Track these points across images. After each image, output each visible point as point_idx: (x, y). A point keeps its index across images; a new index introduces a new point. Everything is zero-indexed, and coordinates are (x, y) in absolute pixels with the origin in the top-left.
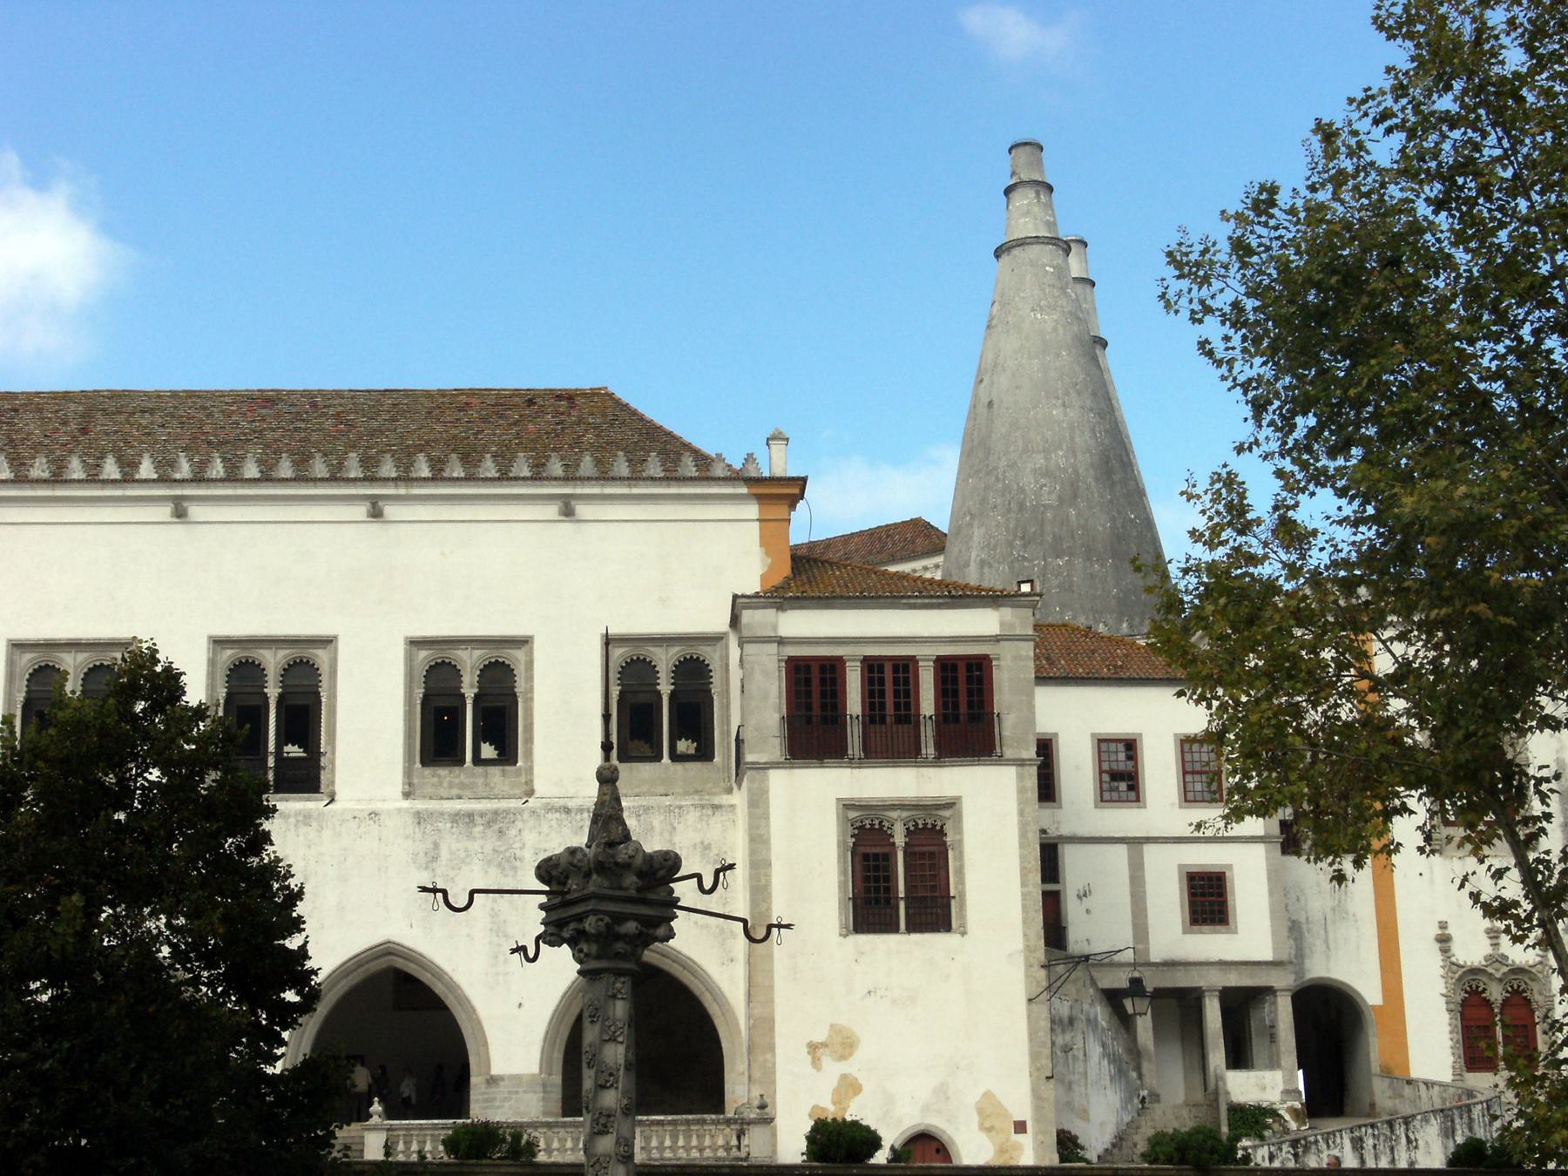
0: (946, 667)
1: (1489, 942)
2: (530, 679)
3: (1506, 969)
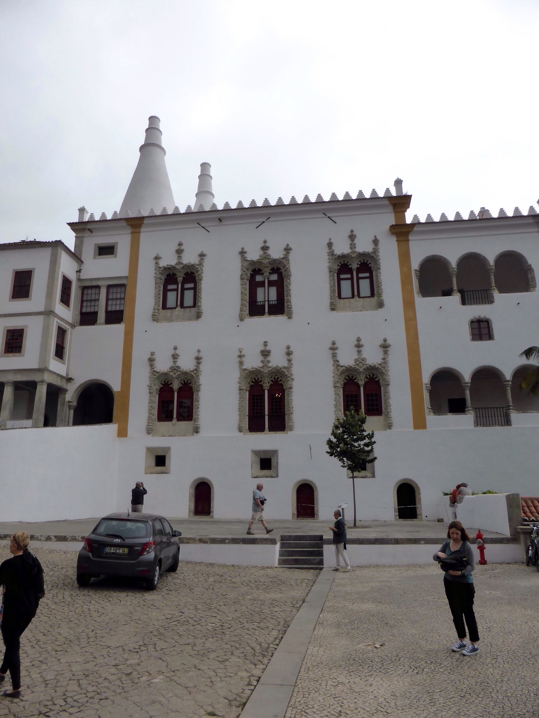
1: (172, 360)
3: (179, 373)
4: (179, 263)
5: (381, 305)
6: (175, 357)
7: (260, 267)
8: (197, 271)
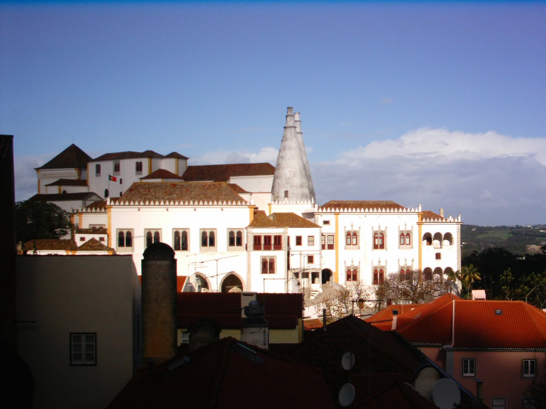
0: (275, 237)
5: (412, 248)
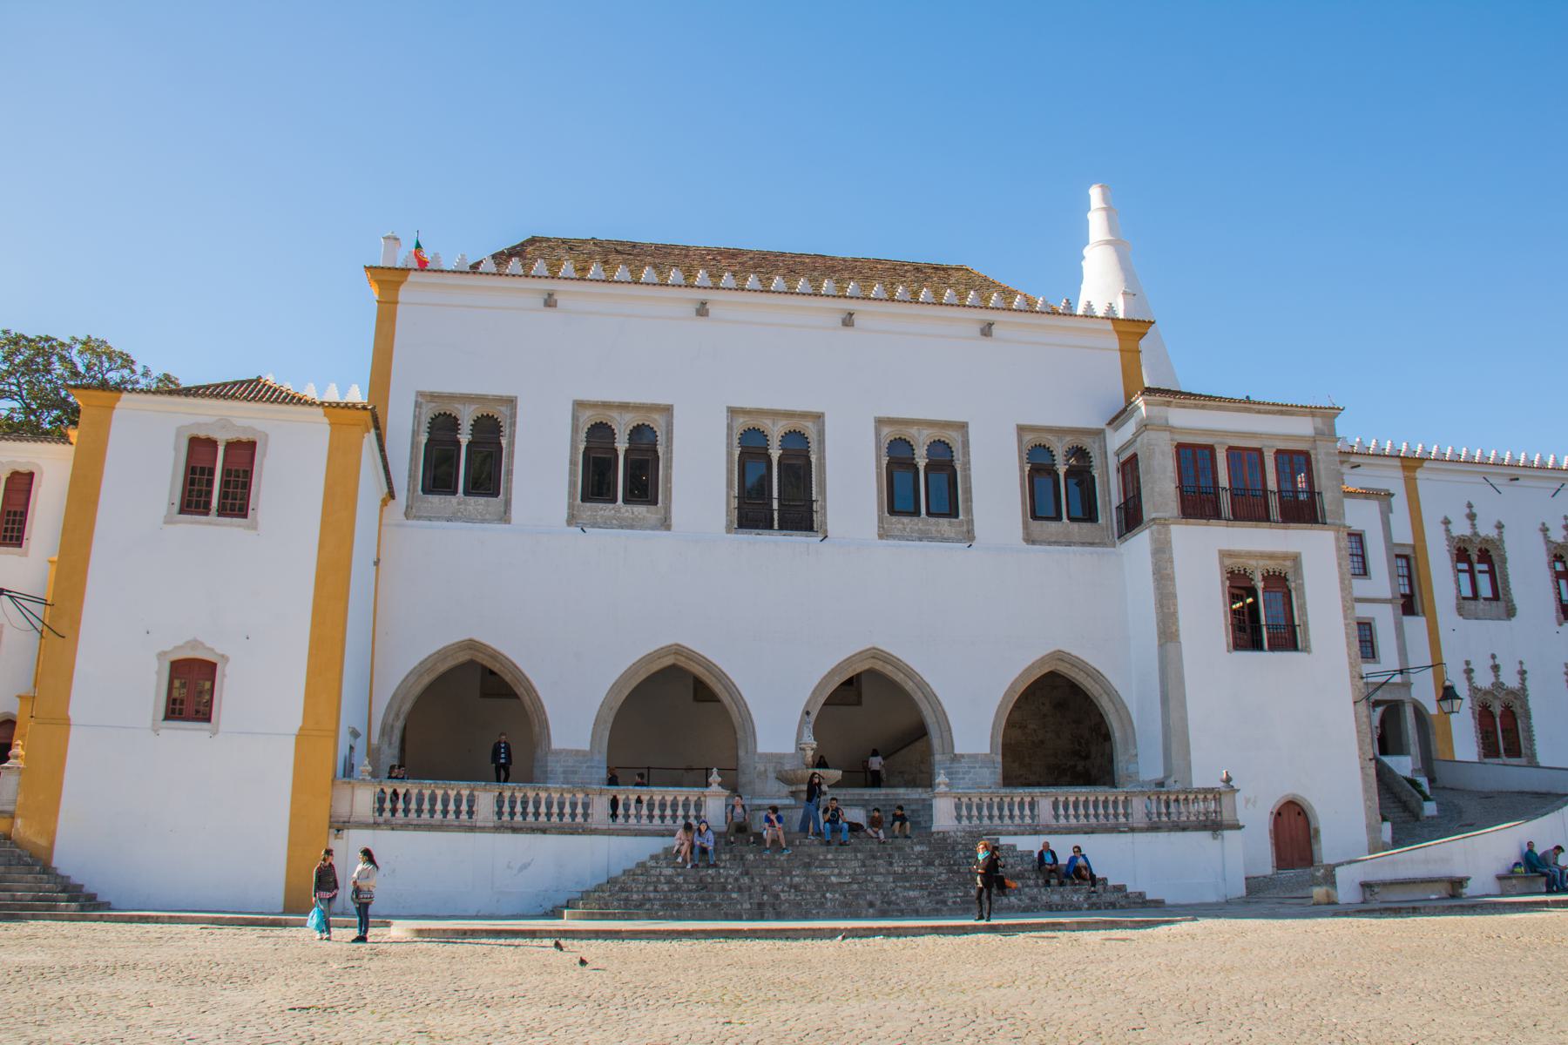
2: (966, 453)
4: (1476, 534)
6: (1496, 668)
7: (1563, 553)
8: (1498, 548)
